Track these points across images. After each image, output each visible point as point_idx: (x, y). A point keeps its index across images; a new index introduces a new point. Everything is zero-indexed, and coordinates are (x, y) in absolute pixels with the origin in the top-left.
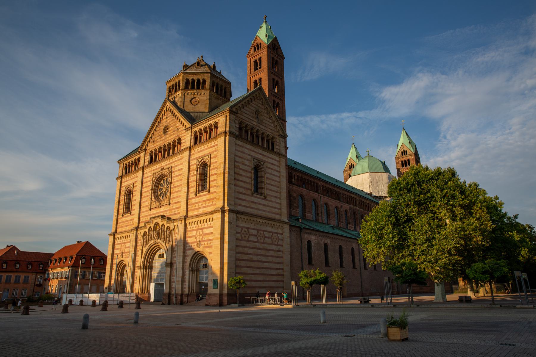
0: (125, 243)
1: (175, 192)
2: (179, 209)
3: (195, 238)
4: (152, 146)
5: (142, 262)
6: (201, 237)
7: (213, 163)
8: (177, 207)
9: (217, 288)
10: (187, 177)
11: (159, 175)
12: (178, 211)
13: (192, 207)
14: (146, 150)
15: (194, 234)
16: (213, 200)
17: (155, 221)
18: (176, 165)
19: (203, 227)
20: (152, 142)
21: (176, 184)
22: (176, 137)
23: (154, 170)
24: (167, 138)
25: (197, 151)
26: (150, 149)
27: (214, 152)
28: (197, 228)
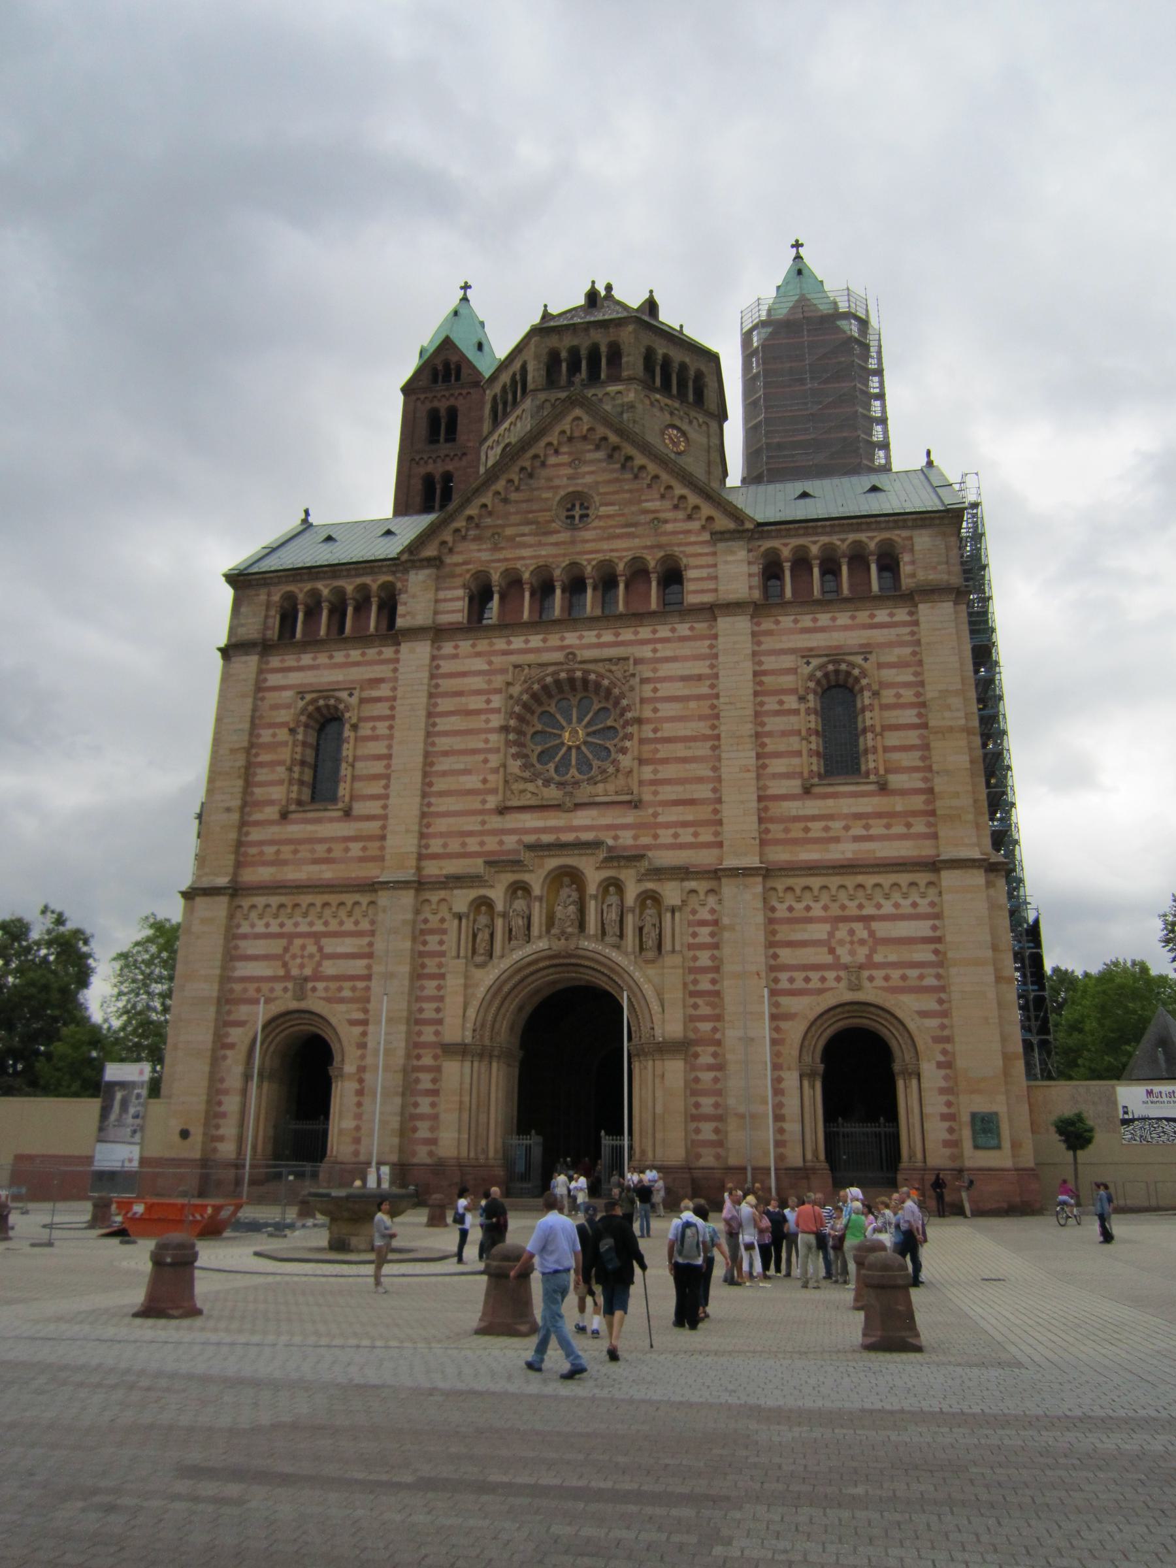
0: (316, 936)
1: (665, 761)
2: (701, 830)
3: (826, 949)
4: (485, 556)
5: (469, 1025)
6: (862, 953)
8: (690, 818)
9: (998, 1147)
10: (750, 712)
11: (549, 679)
12: (696, 835)
13: (787, 830)
14: (442, 562)
15: (825, 936)
16: (911, 820)
17: (553, 863)
18: (658, 655)
19: (869, 911)
20: (477, 539)
21: (668, 730)
22: (646, 547)
23: (505, 653)
24: (587, 541)
25: (792, 625)
26: (465, 563)
27: (890, 645)
28: (835, 910)
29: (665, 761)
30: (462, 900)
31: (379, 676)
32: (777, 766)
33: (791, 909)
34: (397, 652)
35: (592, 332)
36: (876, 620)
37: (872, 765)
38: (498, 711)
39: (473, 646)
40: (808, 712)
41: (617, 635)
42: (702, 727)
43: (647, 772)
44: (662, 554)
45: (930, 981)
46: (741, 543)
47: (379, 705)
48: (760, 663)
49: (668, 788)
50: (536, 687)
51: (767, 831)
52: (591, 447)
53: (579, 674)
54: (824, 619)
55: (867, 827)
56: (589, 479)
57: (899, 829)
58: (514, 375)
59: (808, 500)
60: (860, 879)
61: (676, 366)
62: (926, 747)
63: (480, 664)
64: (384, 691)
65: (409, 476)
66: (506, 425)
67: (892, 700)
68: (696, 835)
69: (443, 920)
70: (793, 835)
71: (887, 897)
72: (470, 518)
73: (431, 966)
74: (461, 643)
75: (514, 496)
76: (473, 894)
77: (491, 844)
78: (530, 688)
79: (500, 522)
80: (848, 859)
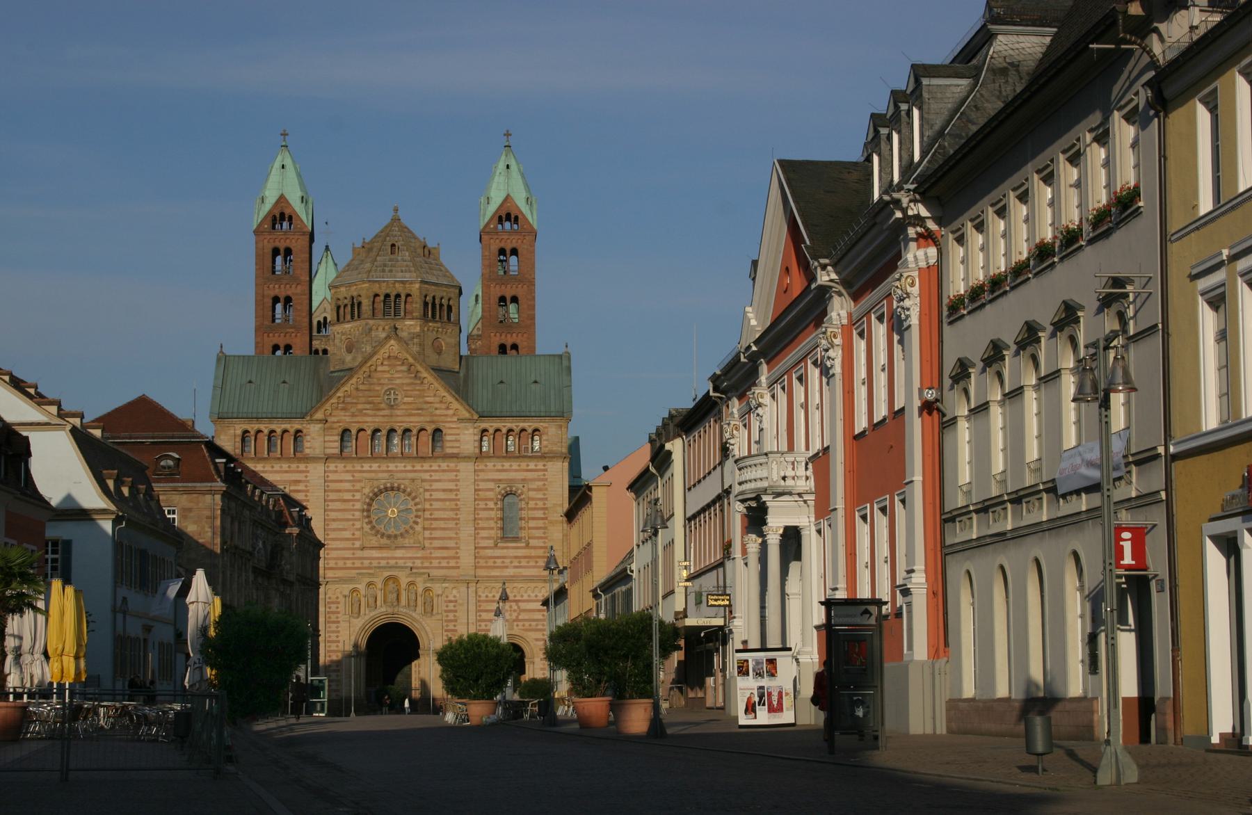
1: (435, 529)
2: (451, 561)
4: (348, 419)
6: (515, 614)
7: (533, 499)
8: (445, 555)
11: (382, 487)
12: (448, 563)
13: (486, 562)
17: (387, 574)
18: (433, 478)
19: (518, 598)
20: (344, 409)
21: (437, 514)
22: (428, 422)
24: (398, 416)
26: (338, 422)
29: (435, 529)
30: (346, 588)
31: (298, 479)
32: (484, 533)
33: (487, 596)
34: (306, 467)
35: (397, 285)
36: (529, 468)
37: (523, 535)
38: (358, 500)
39: (345, 467)
40: (497, 510)
41: (413, 466)
42: (451, 514)
43: (427, 534)
44: (434, 426)
45: (540, 627)
46: (471, 424)
47: (300, 494)
48: (478, 485)
49: (436, 541)
50: (376, 490)
51: (478, 562)
52: (400, 363)
53: (396, 485)
54: (507, 465)
55: (520, 562)
56: (398, 381)
57: (532, 563)
58: (353, 298)
59: (503, 385)
60: (516, 585)
61: (437, 302)
62: (545, 528)
63: (348, 477)
64: (301, 487)
65: (263, 296)
66: (348, 326)
67: (534, 506)
68: (448, 563)
69: (337, 598)
70: (489, 564)
71: (526, 592)
72: (339, 397)
73: (333, 617)
74: (339, 465)
75: (361, 387)
76: (351, 586)
77: (358, 564)
78: (373, 490)
79: (354, 401)
80: (512, 576)
